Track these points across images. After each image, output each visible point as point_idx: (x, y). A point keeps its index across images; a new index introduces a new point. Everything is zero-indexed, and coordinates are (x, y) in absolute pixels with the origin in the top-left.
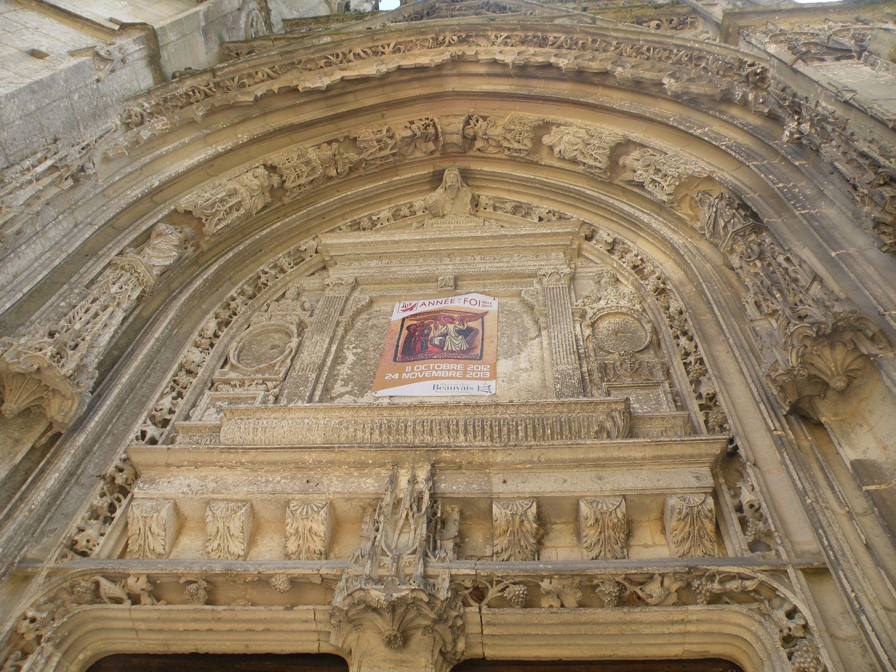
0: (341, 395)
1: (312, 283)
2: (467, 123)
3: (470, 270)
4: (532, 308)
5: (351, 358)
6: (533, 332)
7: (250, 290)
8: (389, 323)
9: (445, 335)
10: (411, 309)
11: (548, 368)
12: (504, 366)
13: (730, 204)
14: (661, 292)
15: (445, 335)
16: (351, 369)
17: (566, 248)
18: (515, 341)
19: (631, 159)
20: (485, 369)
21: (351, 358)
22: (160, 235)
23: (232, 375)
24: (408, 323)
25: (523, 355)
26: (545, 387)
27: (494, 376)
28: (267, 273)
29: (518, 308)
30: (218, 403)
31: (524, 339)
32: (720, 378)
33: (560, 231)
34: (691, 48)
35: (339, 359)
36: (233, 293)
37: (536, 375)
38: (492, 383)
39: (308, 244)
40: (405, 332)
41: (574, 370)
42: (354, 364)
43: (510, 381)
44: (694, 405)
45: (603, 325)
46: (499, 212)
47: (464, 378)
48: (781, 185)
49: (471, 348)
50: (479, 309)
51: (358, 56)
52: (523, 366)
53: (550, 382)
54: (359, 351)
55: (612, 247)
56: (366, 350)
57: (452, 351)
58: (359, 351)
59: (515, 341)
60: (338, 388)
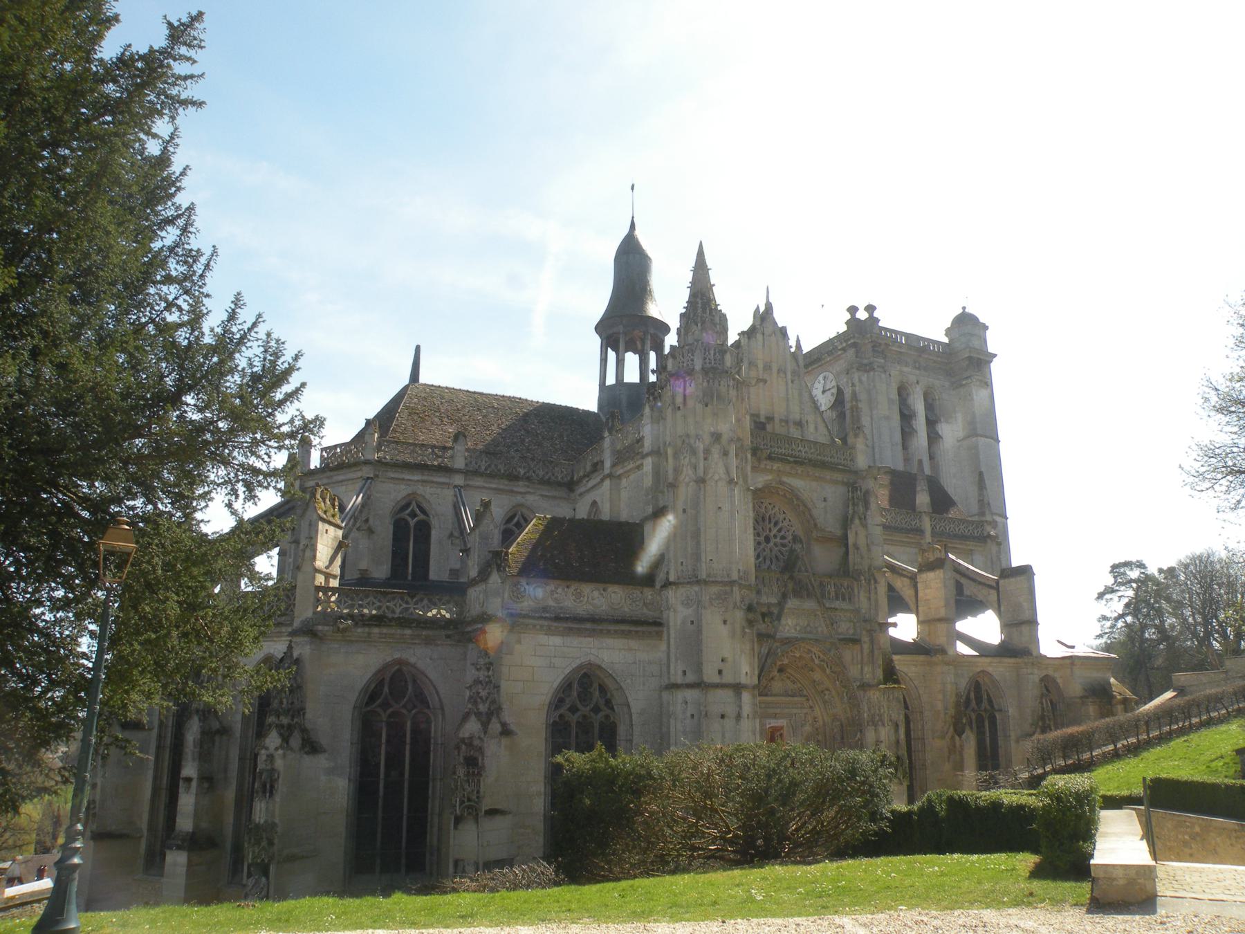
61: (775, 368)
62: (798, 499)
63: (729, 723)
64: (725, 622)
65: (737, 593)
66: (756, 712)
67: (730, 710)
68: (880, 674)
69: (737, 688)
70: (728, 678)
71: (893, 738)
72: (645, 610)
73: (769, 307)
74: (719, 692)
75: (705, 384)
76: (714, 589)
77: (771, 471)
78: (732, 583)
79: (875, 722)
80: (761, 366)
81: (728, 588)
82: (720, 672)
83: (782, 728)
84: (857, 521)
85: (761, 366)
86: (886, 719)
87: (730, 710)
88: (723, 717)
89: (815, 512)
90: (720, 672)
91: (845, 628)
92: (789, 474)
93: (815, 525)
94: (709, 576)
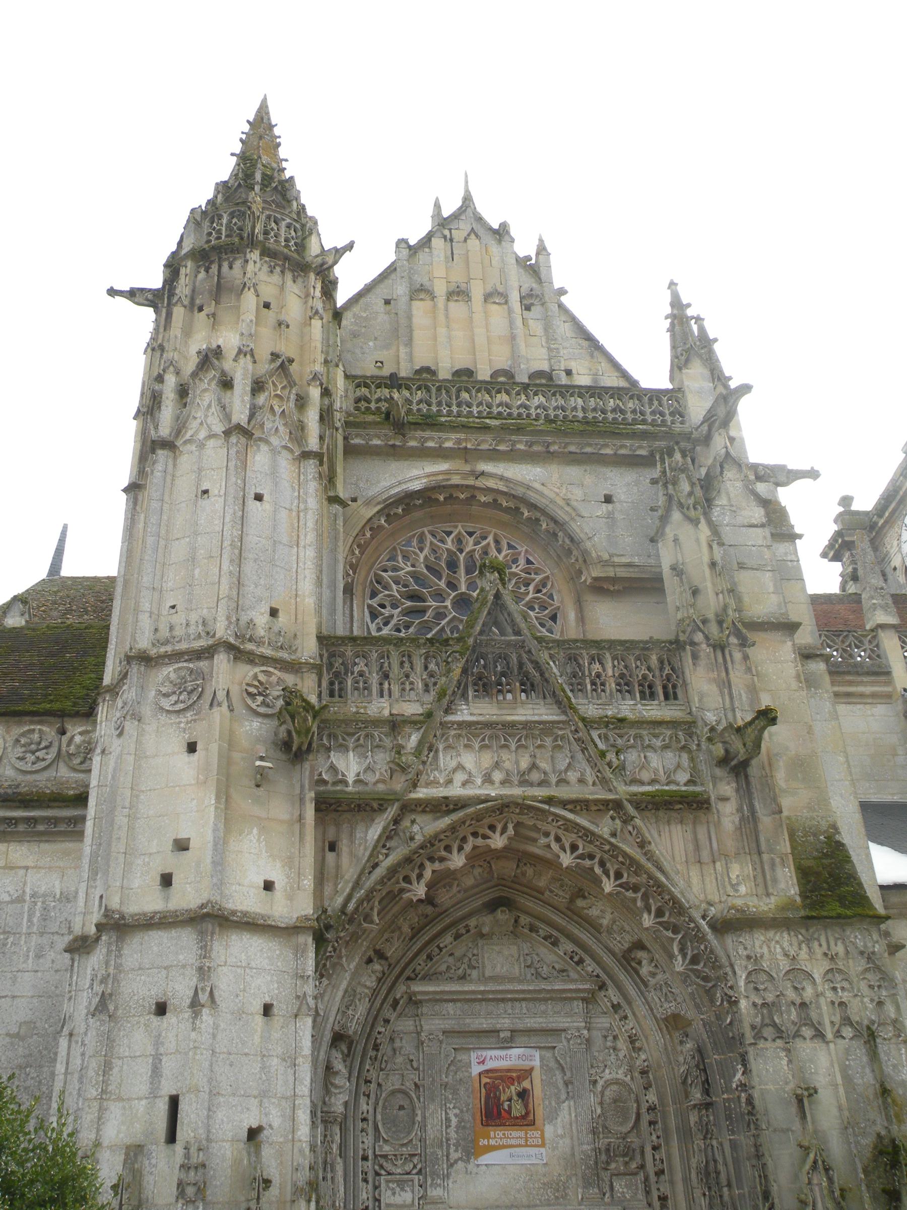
0: (456, 1161)
1: (407, 1025)
2: (518, 866)
3: (520, 1026)
4: (563, 1069)
5: (454, 1121)
6: (563, 1096)
7: (373, 1053)
8: (470, 1077)
9: (510, 1100)
10: (483, 1062)
11: (576, 1143)
12: (549, 1130)
13: (697, 1066)
14: (644, 1072)
15: (510, 1100)
16: (457, 1132)
17: (583, 999)
18: (553, 1103)
19: (641, 954)
20: (537, 1134)
21: (454, 1121)
22: (337, 1073)
23: (387, 1148)
24: (485, 1080)
25: (559, 1119)
26: (573, 1155)
27: (543, 1145)
28: (379, 1033)
29: (552, 1064)
30: (391, 1185)
31: (559, 1102)
32: (672, 1182)
33: (581, 987)
34: (697, 926)
35: (448, 1120)
36: (367, 1067)
37: (567, 1141)
38: (542, 1150)
39: (401, 989)
40: (483, 1090)
41: (592, 1150)
42: (457, 1127)
43: (554, 1149)
44: (655, 1194)
45: (607, 1093)
46: (534, 935)
47: (527, 1146)
48: (725, 1096)
49: (527, 1114)
50: (526, 1064)
51: (440, 841)
52: (560, 1131)
53: (577, 1157)
54: (457, 1111)
55: (616, 1007)
56: (462, 1111)
57: (517, 1118)
58: (457, 1111)
59: (553, 1103)
60: (454, 1155)
61: (477, 292)
62: (533, 506)
63: (174, 1025)
64: (192, 748)
65: (225, 674)
66: (301, 998)
67: (181, 989)
68: (787, 885)
69: (212, 920)
70: (188, 895)
71: (865, 1079)
72: (64, 772)
73: (467, 199)
74: (157, 940)
75: (202, 275)
76: (169, 671)
77: (440, 454)
78: (207, 653)
79: (791, 1025)
80: (440, 289)
81: (203, 664)
82: (167, 880)
83: (527, 1073)
84: (676, 516)
85: (440, 289)
86: (827, 1016)
87: (181, 989)
88: (161, 1009)
89: (580, 528)
90: (167, 880)
91: (659, 766)
92: (494, 455)
93: (585, 554)
94: (157, 643)
